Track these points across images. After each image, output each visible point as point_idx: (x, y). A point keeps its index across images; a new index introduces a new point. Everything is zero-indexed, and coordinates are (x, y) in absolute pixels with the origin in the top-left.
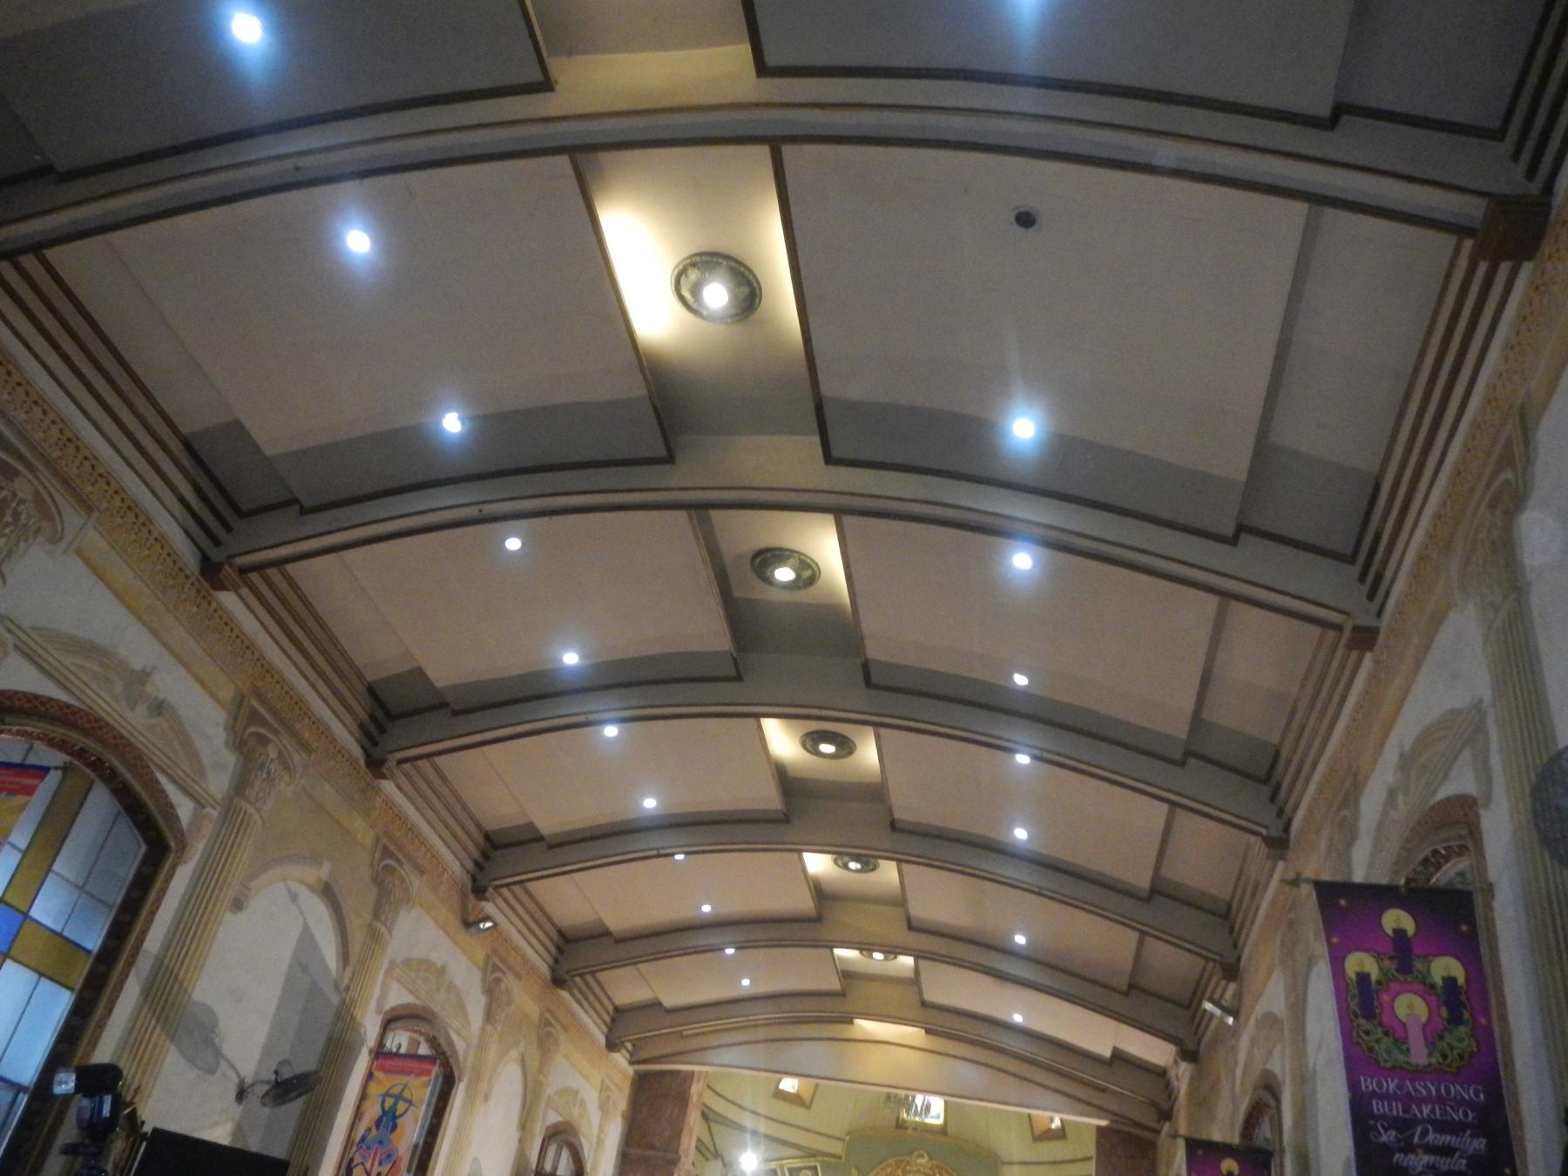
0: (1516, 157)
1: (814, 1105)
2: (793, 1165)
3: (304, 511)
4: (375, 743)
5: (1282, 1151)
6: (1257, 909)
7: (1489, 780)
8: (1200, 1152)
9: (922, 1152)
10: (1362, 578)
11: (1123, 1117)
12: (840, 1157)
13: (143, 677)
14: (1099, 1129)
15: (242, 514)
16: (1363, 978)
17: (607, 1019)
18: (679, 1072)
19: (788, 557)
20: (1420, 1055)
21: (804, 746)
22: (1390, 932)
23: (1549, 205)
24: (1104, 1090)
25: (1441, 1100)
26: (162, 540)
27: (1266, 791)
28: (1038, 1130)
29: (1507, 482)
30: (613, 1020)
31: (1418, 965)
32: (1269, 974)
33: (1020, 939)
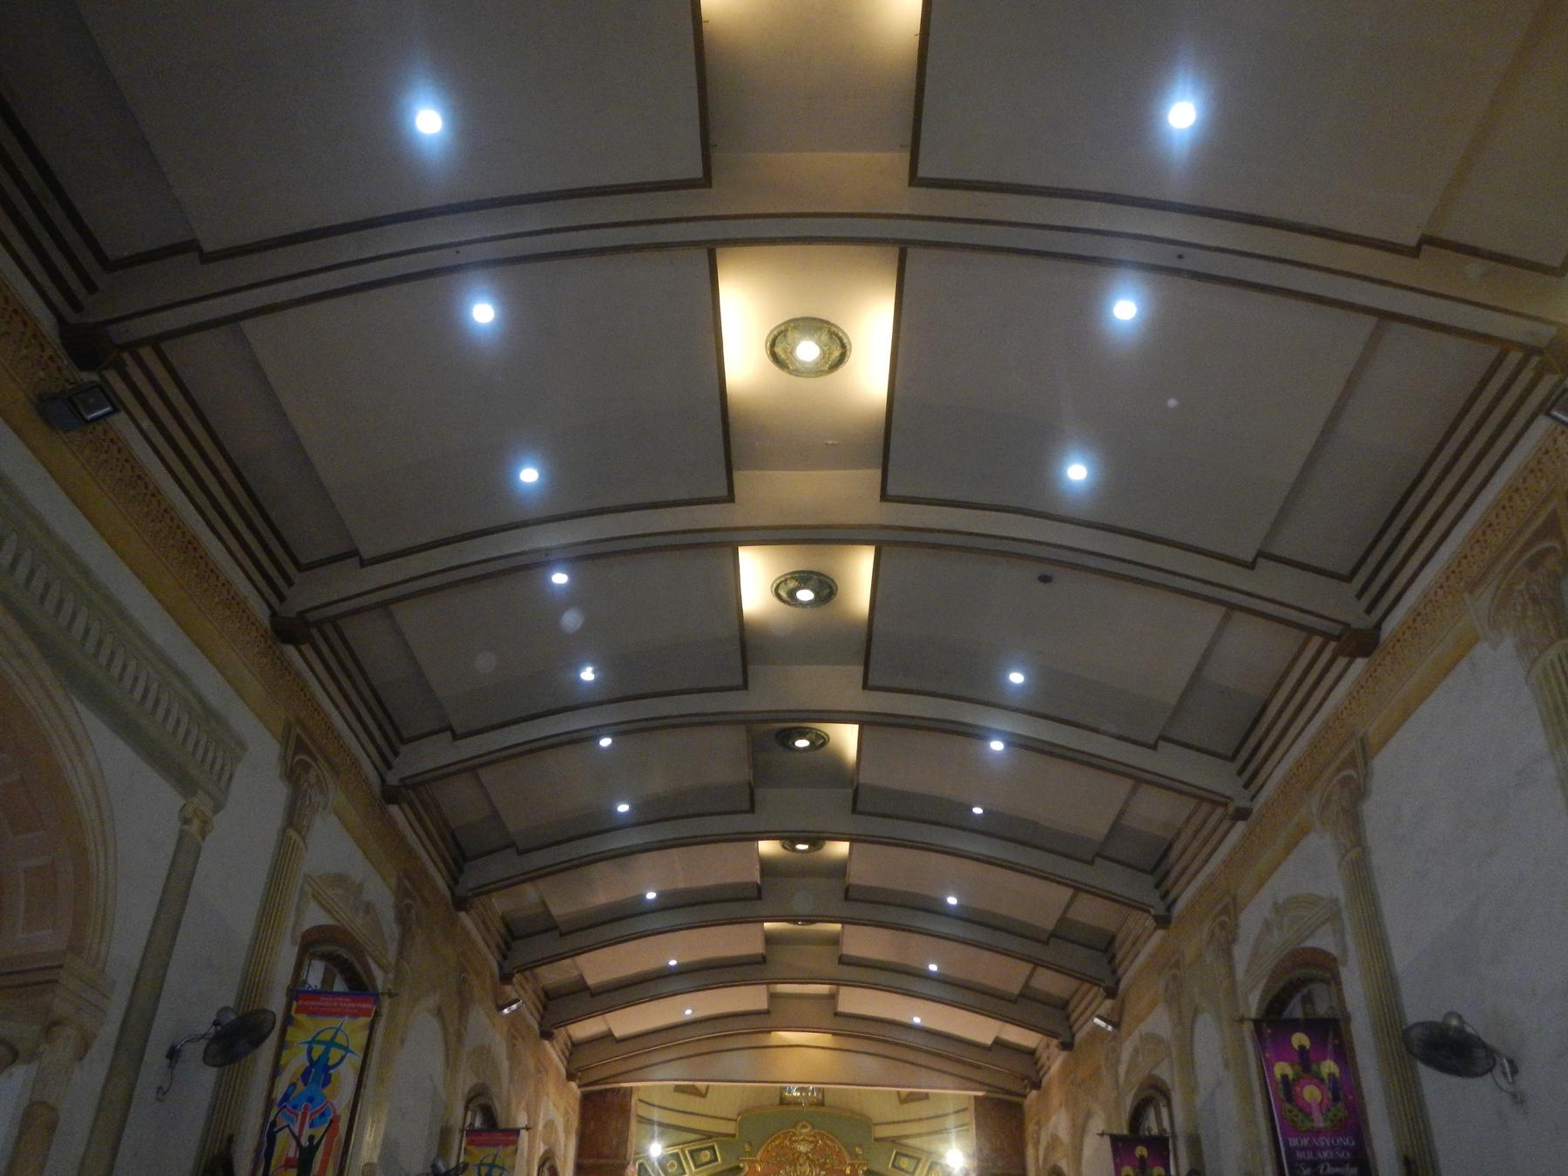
0: (1359, 596)
1: (709, 1094)
2: (694, 1147)
3: (456, 737)
4: (455, 880)
5: (1174, 1136)
6: (1137, 955)
7: (1345, 950)
8: (1120, 1144)
9: (804, 1123)
10: (1240, 773)
11: (996, 1087)
12: (734, 1136)
14: (976, 1098)
15: (404, 741)
16: (1285, 1077)
18: (619, 1089)
19: (808, 733)
20: (1320, 1122)
21: (783, 847)
22: (1296, 1047)
23: (1378, 637)
24: (979, 1067)
25: (1333, 1147)
27: (1151, 880)
28: (903, 1097)
30: (571, 1054)
31: (1314, 1067)
33: (933, 967)
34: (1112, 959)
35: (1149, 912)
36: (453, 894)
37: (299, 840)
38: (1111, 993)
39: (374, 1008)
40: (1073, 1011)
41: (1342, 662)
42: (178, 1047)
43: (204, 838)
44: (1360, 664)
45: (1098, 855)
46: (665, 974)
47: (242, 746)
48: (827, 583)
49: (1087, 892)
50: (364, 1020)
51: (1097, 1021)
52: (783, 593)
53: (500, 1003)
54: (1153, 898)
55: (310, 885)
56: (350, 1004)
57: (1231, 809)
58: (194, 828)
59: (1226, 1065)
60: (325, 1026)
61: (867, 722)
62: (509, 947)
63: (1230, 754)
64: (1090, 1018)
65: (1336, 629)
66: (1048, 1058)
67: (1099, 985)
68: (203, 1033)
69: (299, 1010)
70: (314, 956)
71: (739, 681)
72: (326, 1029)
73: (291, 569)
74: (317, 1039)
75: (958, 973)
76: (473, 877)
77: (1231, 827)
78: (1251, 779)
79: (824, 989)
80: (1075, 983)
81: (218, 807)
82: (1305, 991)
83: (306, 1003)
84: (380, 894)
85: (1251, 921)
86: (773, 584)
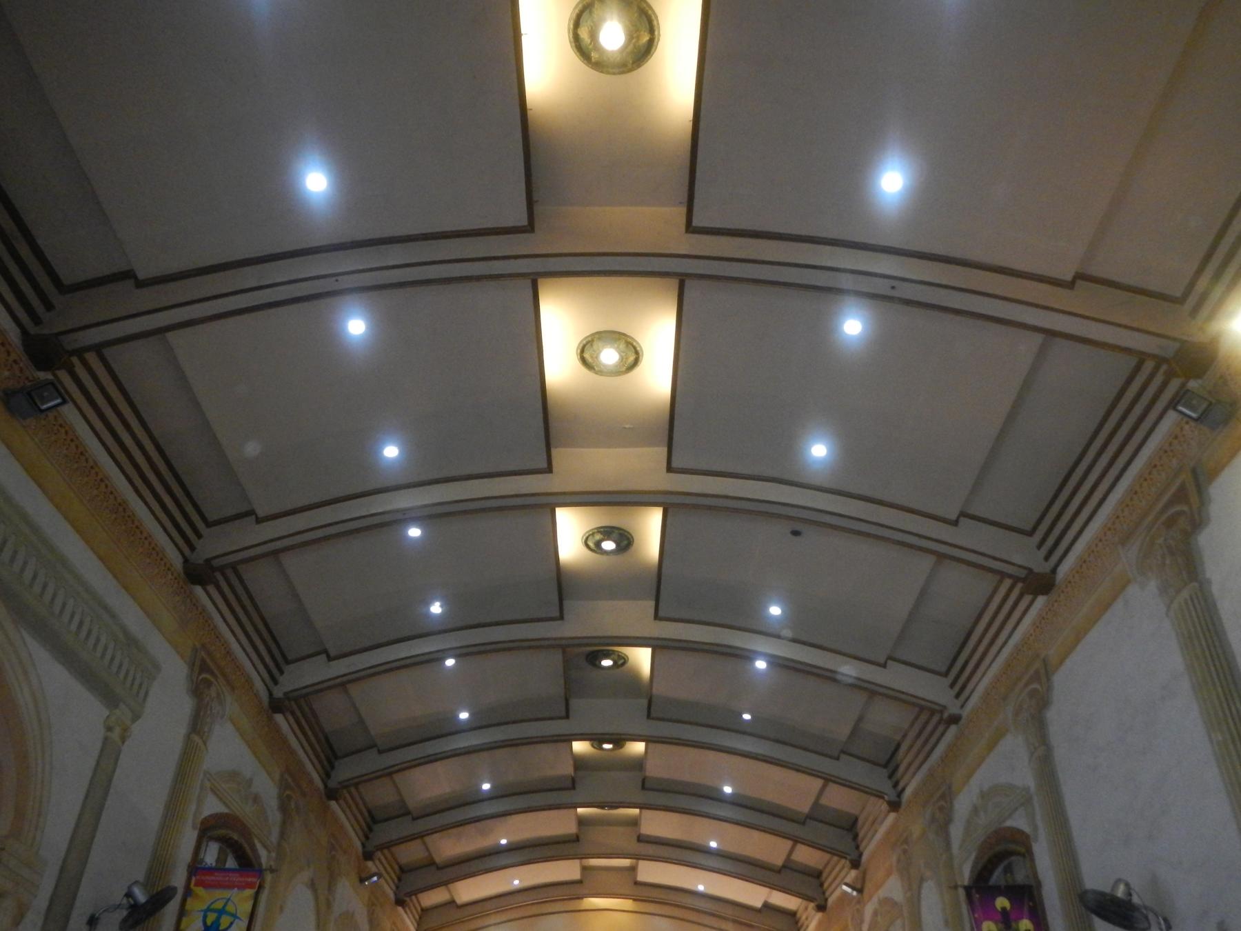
0: (1039, 546)
3: (330, 658)
4: (328, 775)
7: (1035, 828)
10: (952, 686)
13: (250, 782)
15: (288, 662)
17: (417, 917)
21: (593, 746)
22: (1000, 909)
26: (256, 695)
27: (885, 772)
29: (1035, 690)
30: (420, 918)
31: (1014, 925)
32: (889, 874)
33: (713, 844)
34: (855, 837)
35: (883, 798)
36: (326, 786)
37: (200, 742)
38: (856, 864)
39: (258, 883)
40: (826, 878)
41: (1027, 598)
42: (97, 915)
43: (123, 742)
44: (1041, 600)
45: (843, 752)
46: (498, 851)
47: (157, 667)
48: (626, 536)
49: (835, 782)
50: (249, 892)
51: (845, 887)
52: (591, 544)
53: (363, 875)
54: (886, 787)
55: (209, 780)
56: (235, 878)
57: (946, 715)
58: (115, 735)
59: (946, 923)
60: (217, 897)
61: (659, 647)
62: (371, 830)
63: (944, 669)
64: (839, 885)
65: (1023, 573)
66: (807, 919)
67: (846, 858)
68: (118, 903)
69: (197, 884)
70: (211, 839)
71: (557, 614)
72: (218, 899)
73: (200, 525)
74: (212, 907)
75: (733, 848)
76: (346, 771)
77: (947, 728)
78: (961, 690)
79: (626, 862)
80: (828, 856)
81: (136, 717)
82: (1006, 863)
83: (203, 878)
84: (267, 788)
85: (963, 804)
86: (583, 537)
